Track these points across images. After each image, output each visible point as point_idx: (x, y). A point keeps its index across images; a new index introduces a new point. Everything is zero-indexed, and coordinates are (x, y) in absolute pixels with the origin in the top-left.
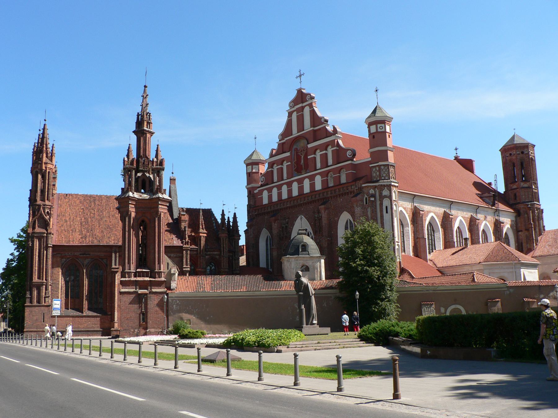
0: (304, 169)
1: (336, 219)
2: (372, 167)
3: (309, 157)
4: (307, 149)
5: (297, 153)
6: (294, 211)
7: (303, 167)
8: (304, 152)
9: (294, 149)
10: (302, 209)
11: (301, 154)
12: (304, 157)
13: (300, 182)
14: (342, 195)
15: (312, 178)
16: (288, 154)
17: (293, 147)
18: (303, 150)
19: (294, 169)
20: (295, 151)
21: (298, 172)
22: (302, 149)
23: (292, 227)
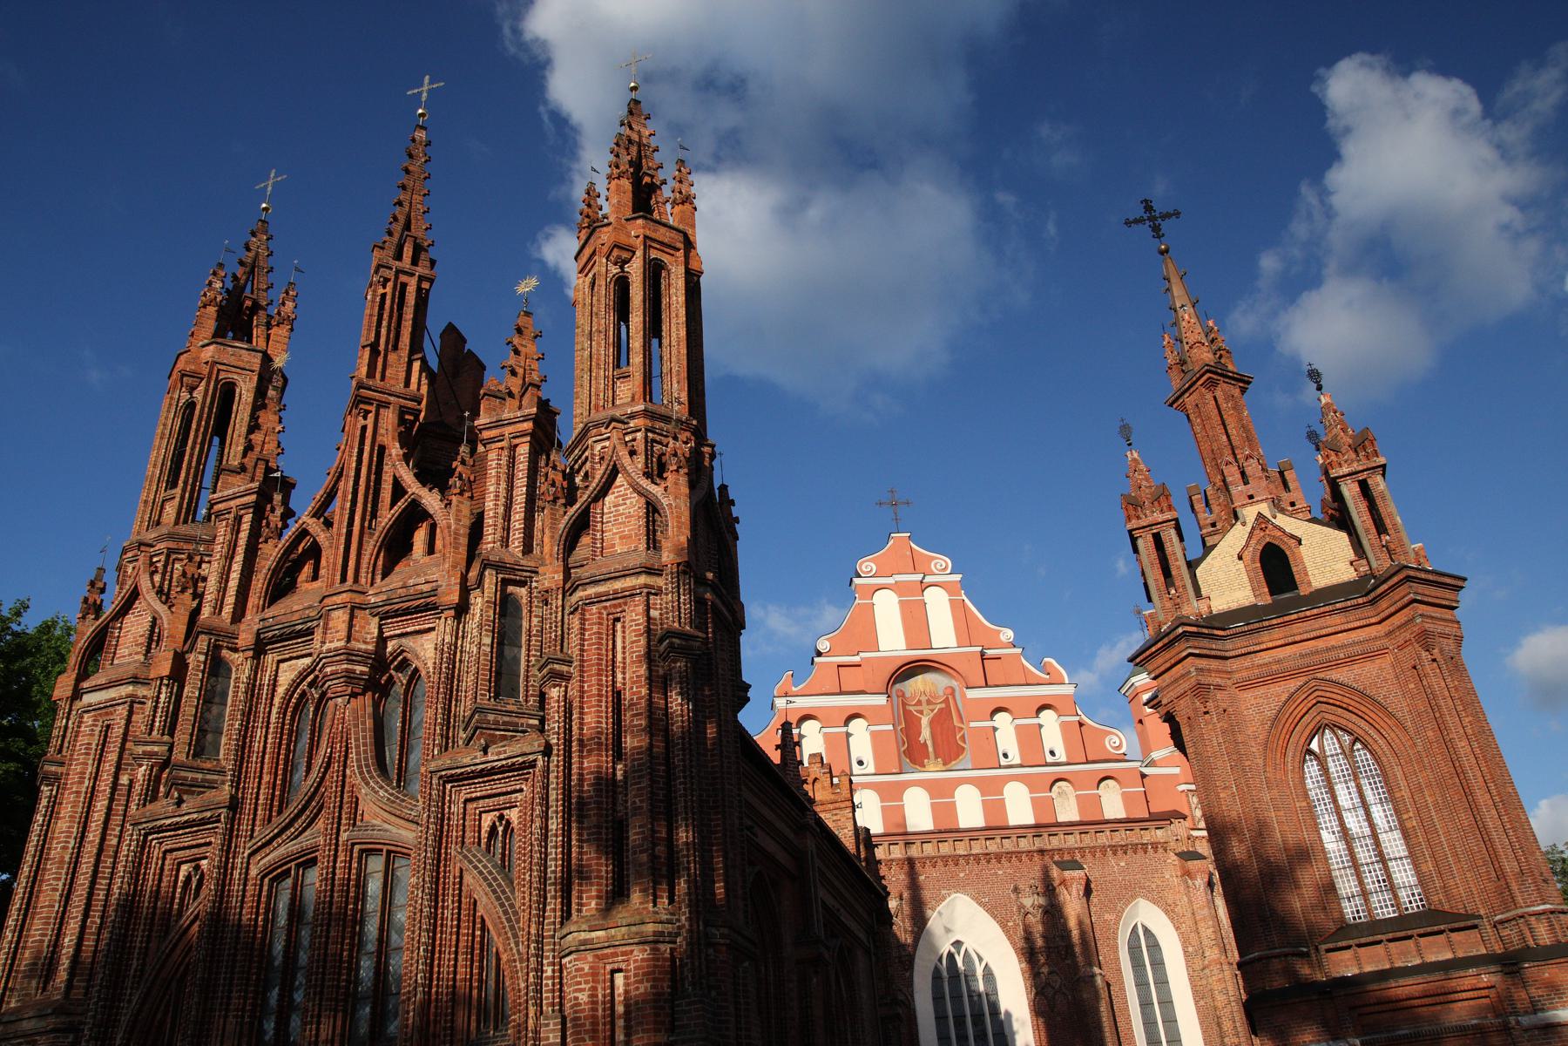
0: (936, 758)
1: (1107, 916)
3: (972, 724)
4: (946, 701)
5: (904, 704)
7: (931, 749)
8: (931, 707)
9: (898, 690)
10: (962, 875)
11: (921, 712)
12: (932, 723)
13: (941, 793)
15: (991, 790)
16: (881, 700)
18: (924, 704)
19: (902, 749)
20: (898, 697)
21: (913, 761)
22: (924, 699)
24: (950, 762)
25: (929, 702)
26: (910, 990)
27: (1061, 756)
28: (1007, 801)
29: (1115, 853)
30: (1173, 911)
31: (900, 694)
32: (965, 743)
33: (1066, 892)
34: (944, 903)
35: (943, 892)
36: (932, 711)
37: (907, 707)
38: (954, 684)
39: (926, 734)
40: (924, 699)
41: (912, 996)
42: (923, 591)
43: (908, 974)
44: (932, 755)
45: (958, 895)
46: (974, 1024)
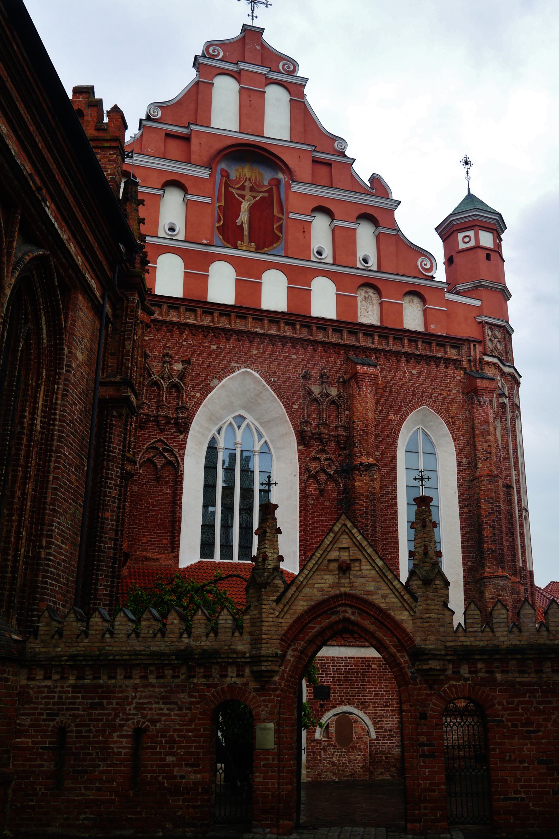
0: (250, 241)
2: (486, 323)
3: (291, 216)
4: (270, 191)
5: (227, 185)
6: (214, 347)
7: (246, 233)
8: (254, 194)
9: (223, 170)
10: (255, 352)
11: (243, 197)
12: (251, 209)
14: (419, 358)
16: (204, 174)
17: (218, 163)
18: (247, 190)
19: (217, 225)
22: (248, 184)
23: (198, 395)
24: (264, 248)
25: (252, 189)
26: (181, 452)
27: (373, 264)
28: (313, 293)
29: (408, 362)
30: (454, 423)
31: (225, 174)
32: (281, 232)
33: (355, 386)
34: (231, 376)
35: (233, 364)
36: (254, 197)
37: (230, 189)
38: (280, 176)
39: (244, 217)
40: (248, 184)
41: (183, 459)
42: (266, 85)
43: (182, 437)
44: (246, 239)
45: (248, 370)
46: (242, 497)
